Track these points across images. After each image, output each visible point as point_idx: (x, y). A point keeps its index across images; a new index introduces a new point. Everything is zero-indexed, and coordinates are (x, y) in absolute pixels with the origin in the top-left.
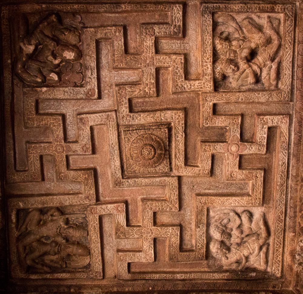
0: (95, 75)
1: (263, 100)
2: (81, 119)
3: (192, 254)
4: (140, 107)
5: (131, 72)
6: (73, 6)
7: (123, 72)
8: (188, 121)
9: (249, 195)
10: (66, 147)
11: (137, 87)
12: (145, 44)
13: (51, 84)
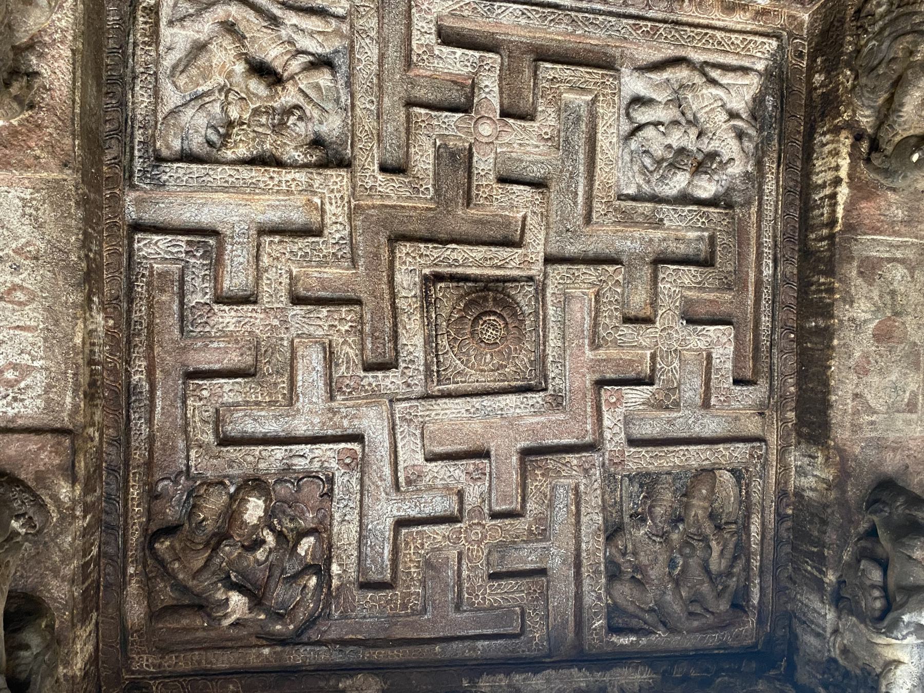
0: (305, 448)
1: (374, 52)
2: (409, 482)
3: (721, 238)
4: (384, 345)
5: (300, 365)
6: (133, 499)
7: (300, 384)
8: (419, 234)
9: (594, 101)
10: (471, 518)
12: (231, 328)
13: (323, 551)
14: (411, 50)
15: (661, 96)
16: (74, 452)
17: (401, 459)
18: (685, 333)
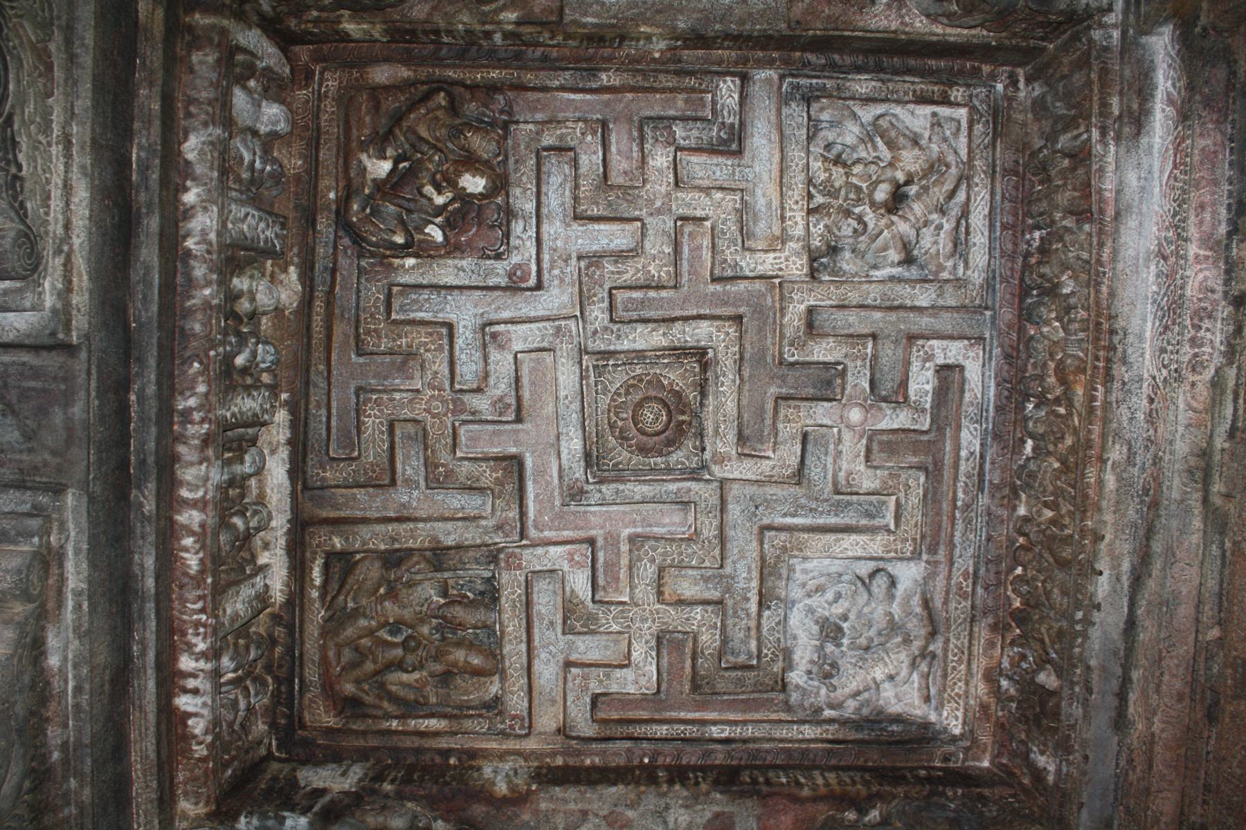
0: (532, 232)
1: (923, 301)
2: (494, 336)
5: (615, 227)
7: (596, 227)
9: (889, 531)
10: (454, 401)
11: (630, 262)
14: (928, 339)
15: (896, 609)
16: (542, 24)
17: (519, 326)
18: (649, 637)
